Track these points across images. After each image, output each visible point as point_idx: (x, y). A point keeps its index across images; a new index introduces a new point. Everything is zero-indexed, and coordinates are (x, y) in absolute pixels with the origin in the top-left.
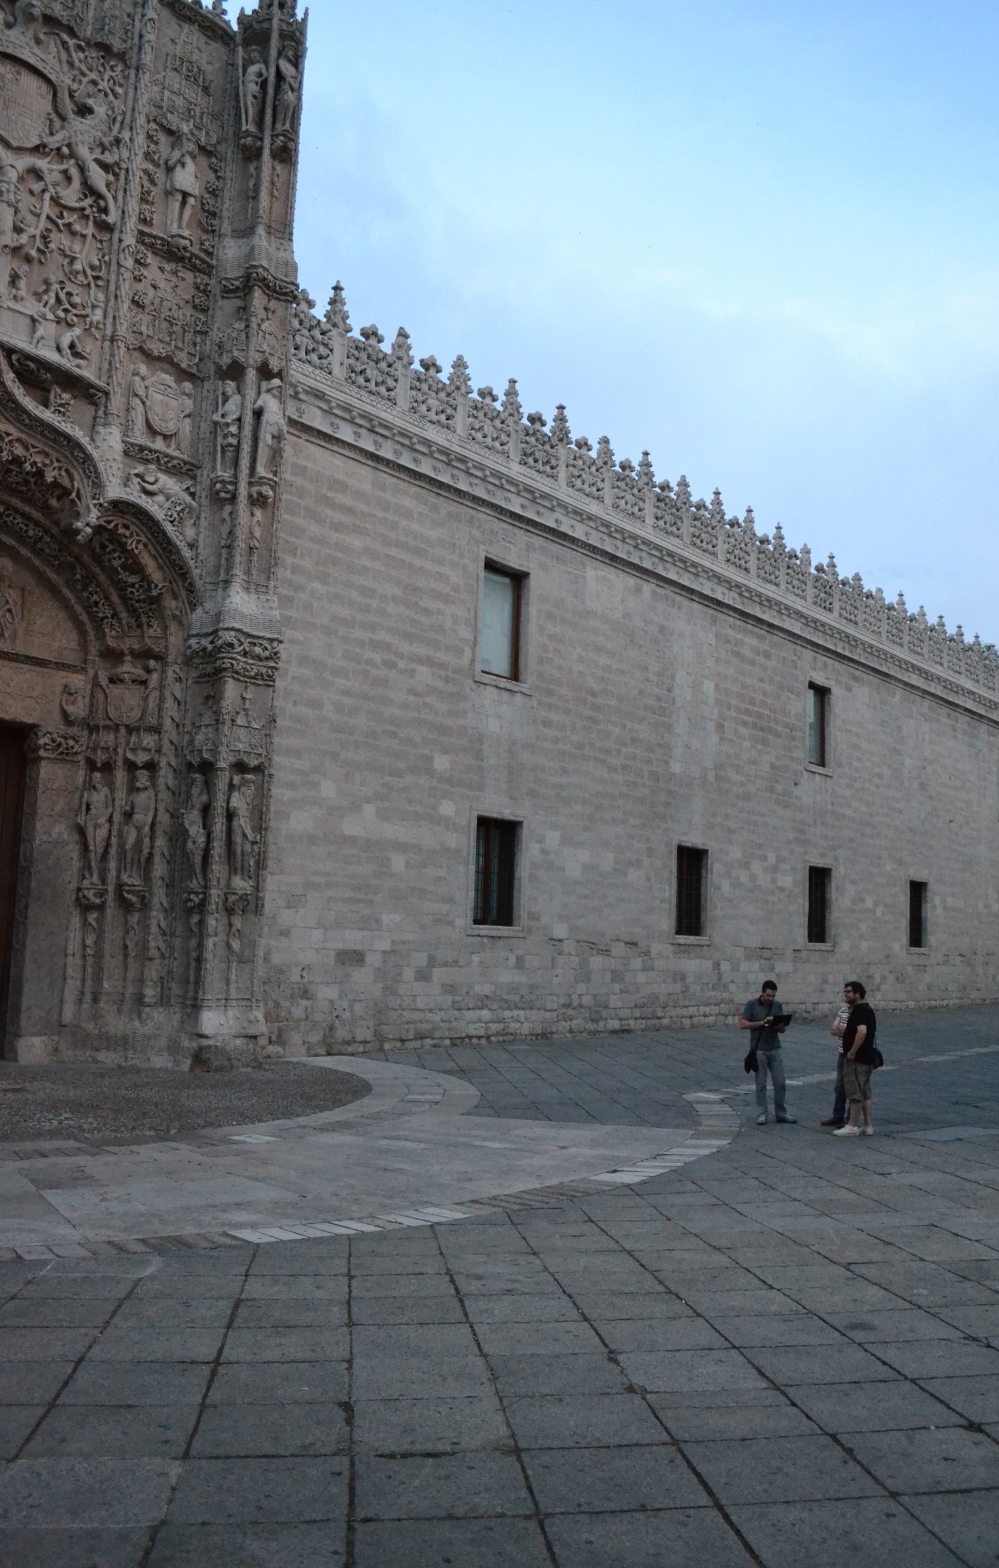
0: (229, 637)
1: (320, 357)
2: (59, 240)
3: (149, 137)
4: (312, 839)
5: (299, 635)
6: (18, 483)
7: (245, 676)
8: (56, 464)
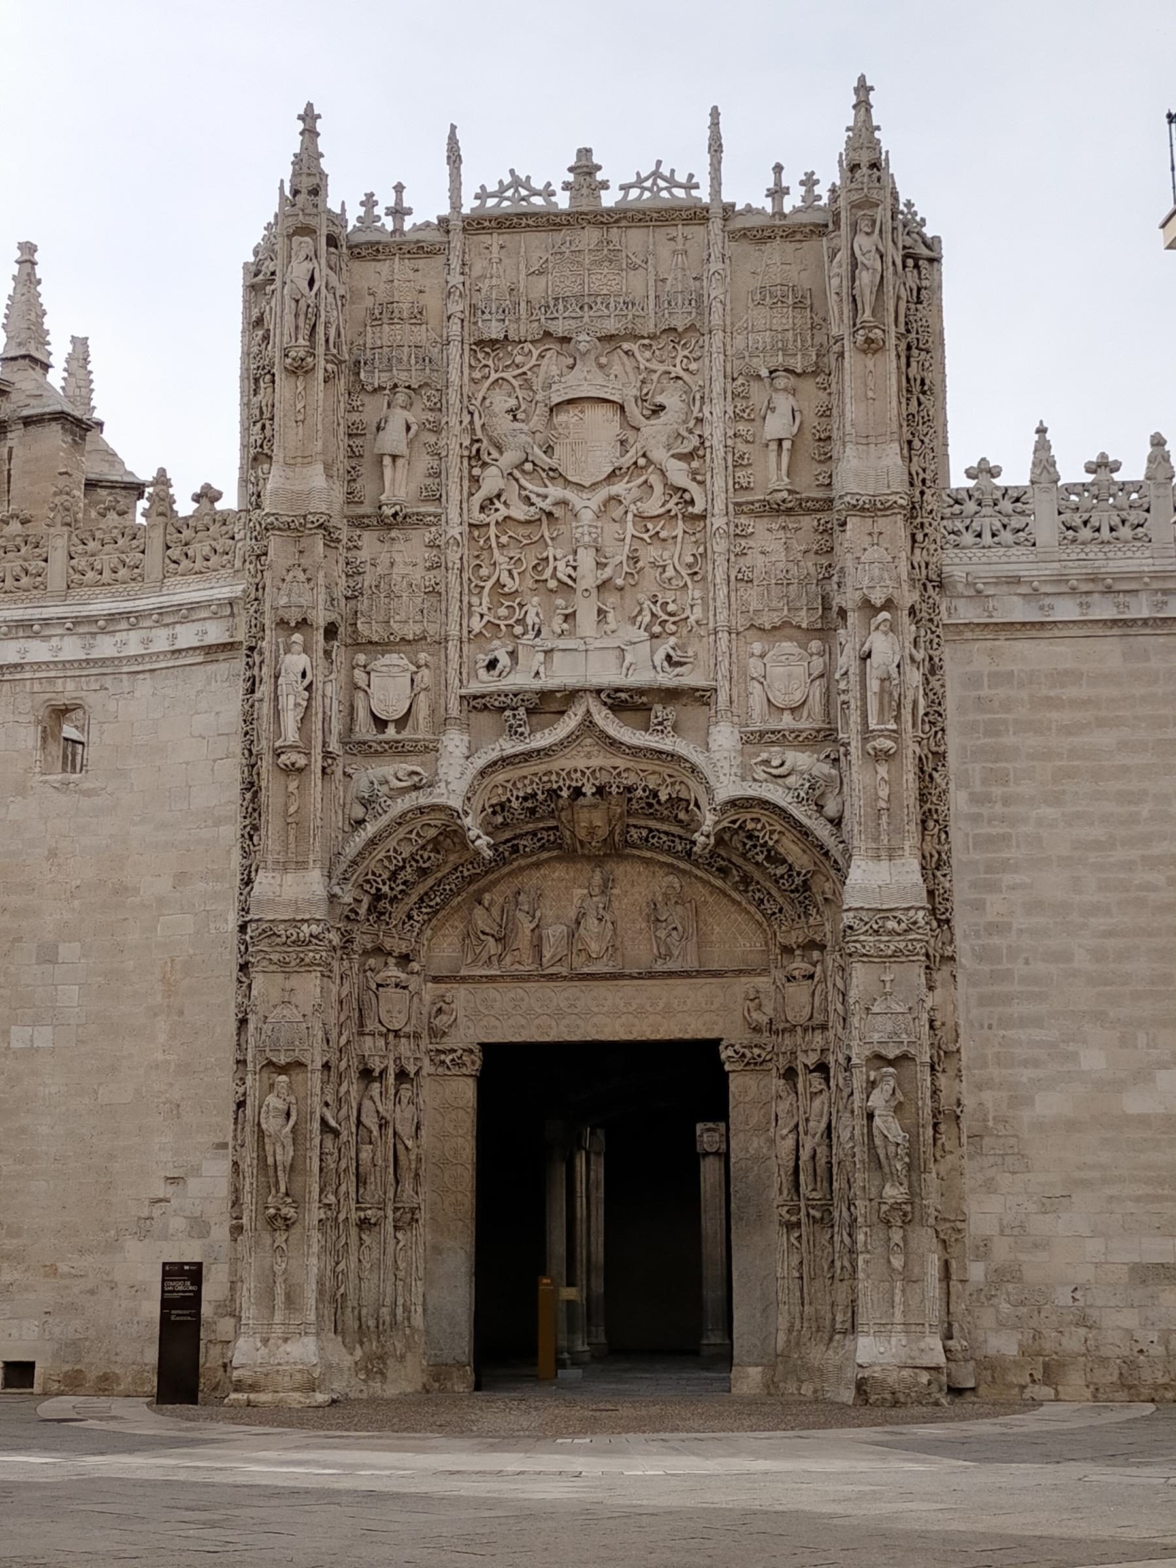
0: (848, 918)
4: (1072, 1125)
6: (642, 808)
7: (881, 957)
8: (669, 780)
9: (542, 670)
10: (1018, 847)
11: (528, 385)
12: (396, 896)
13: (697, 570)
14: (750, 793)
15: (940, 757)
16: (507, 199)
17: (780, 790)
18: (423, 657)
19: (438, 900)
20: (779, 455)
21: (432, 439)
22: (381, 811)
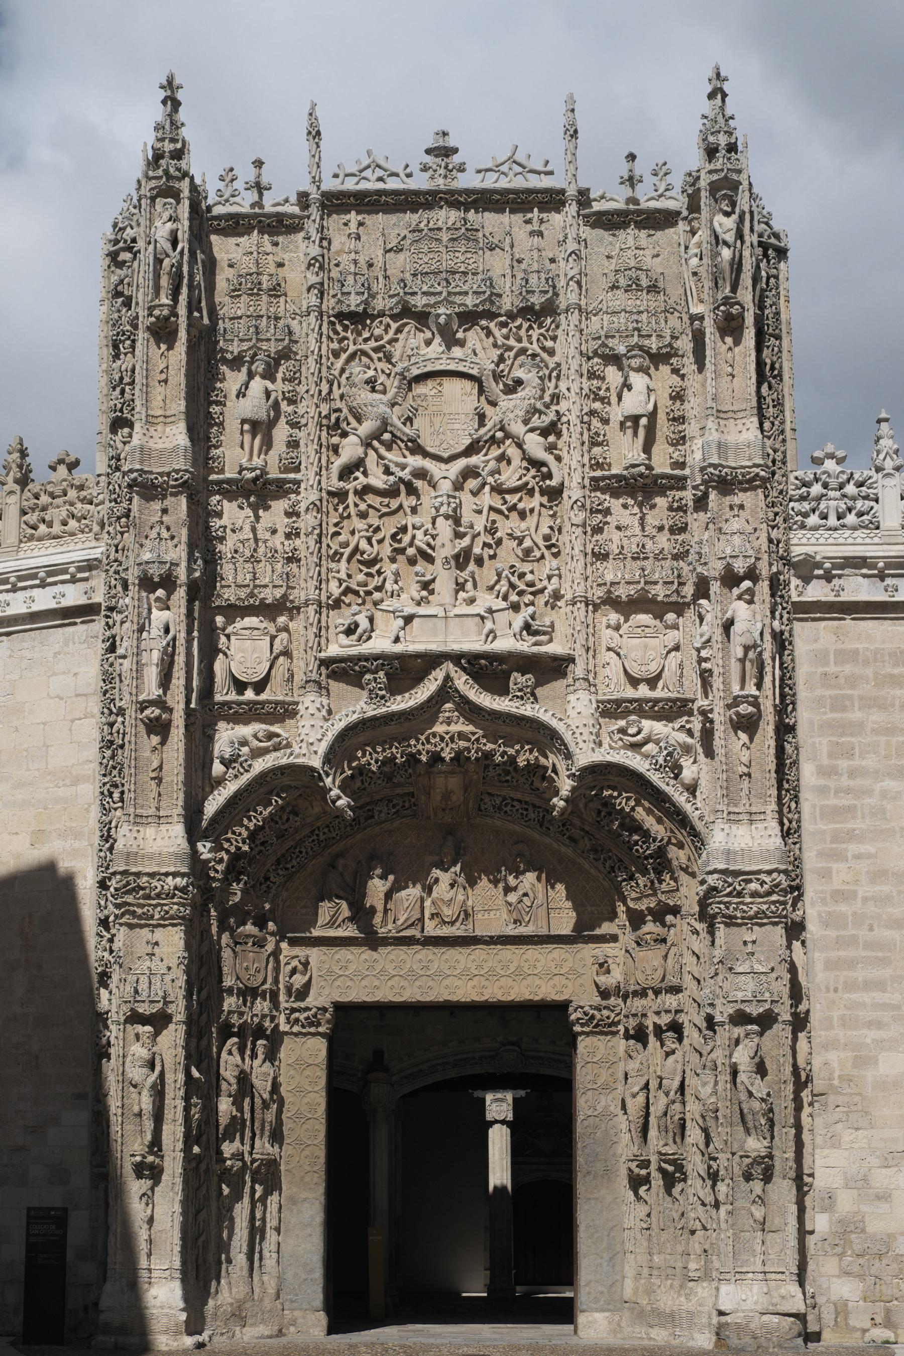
1: (860, 514)
2: (508, 525)
3: (592, 375)
5: (868, 847)
9: (402, 634)
10: (863, 818)
11: (388, 358)
12: (254, 857)
13: (554, 541)
14: (609, 758)
15: (791, 729)
16: (364, 178)
17: (639, 757)
18: (282, 620)
19: (294, 862)
20: (635, 434)
21: (290, 409)
22: (242, 770)
